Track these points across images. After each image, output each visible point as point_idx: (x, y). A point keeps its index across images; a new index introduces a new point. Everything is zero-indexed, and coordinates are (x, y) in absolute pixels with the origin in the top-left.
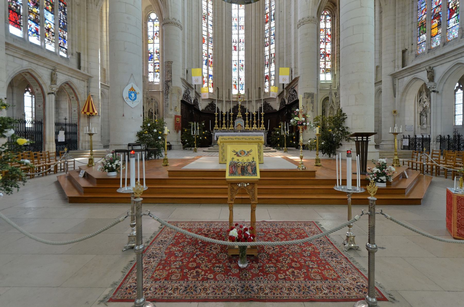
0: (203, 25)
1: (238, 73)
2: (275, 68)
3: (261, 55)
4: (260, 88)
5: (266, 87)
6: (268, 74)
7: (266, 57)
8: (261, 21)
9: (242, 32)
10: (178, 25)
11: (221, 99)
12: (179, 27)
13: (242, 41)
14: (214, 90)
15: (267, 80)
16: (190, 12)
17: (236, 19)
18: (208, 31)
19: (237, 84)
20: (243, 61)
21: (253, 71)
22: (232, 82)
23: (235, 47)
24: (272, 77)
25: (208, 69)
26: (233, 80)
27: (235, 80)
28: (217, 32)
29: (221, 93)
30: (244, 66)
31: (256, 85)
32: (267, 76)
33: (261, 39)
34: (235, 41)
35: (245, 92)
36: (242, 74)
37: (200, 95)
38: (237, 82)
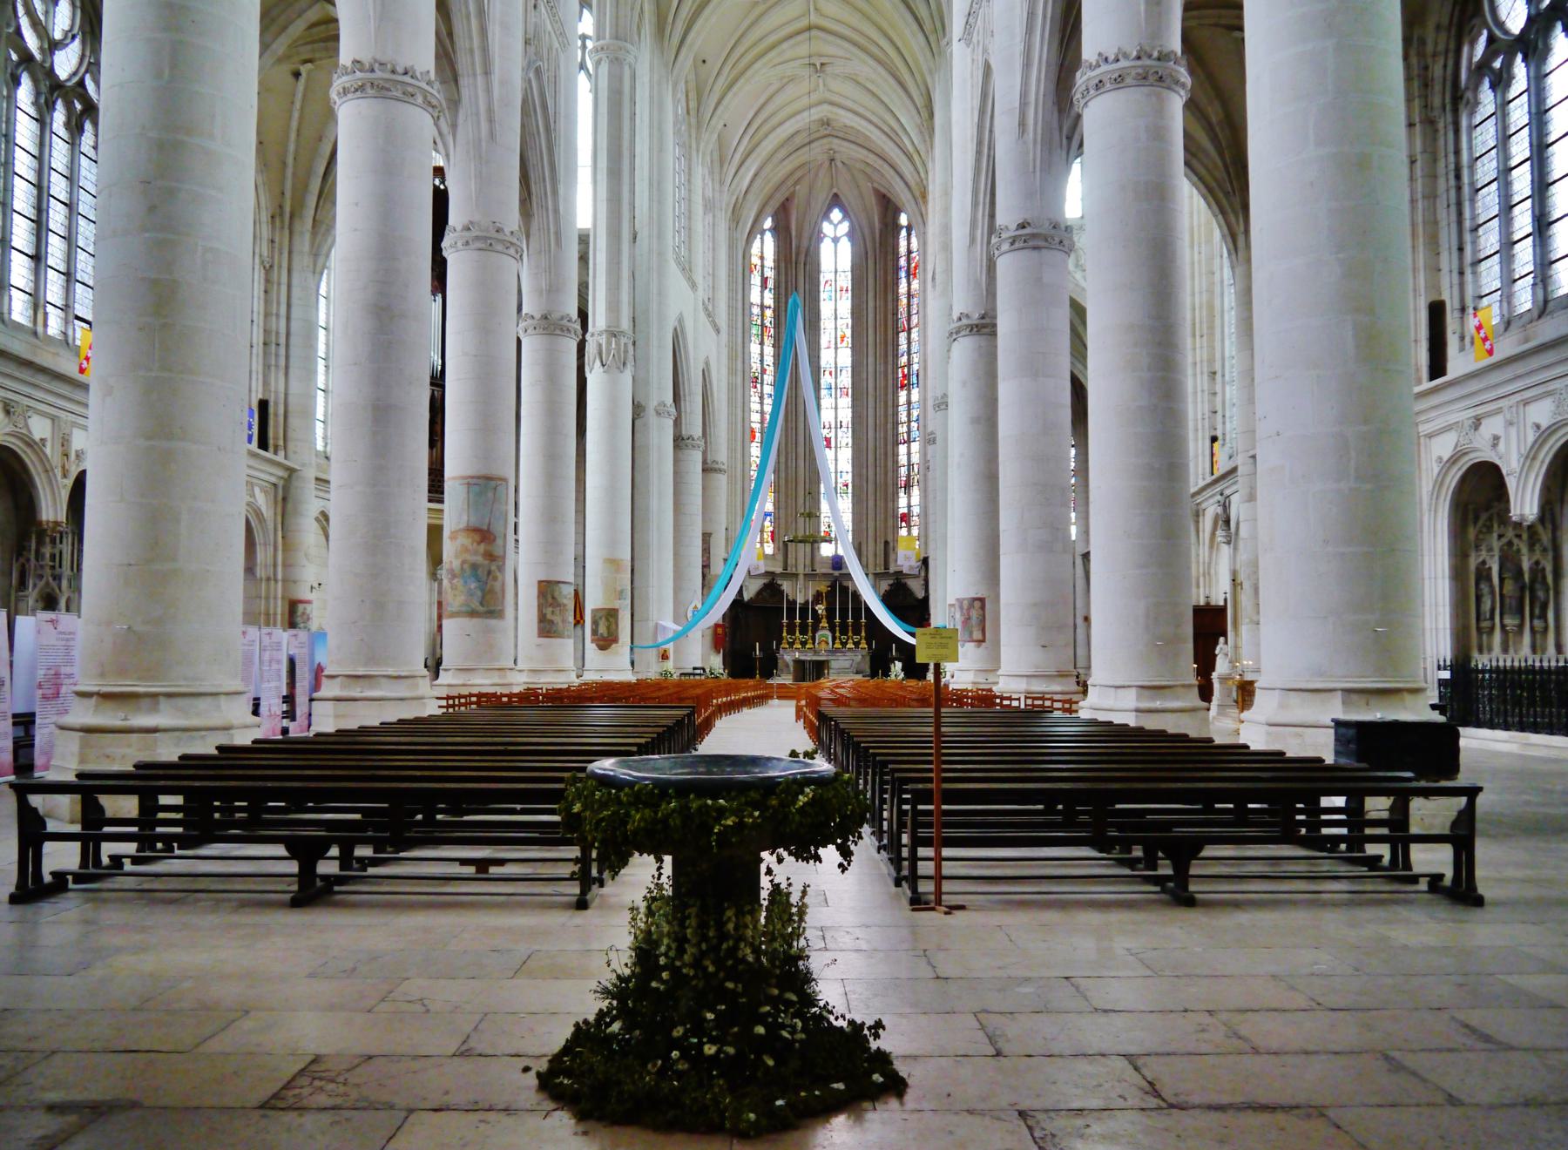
0: (753, 399)
3: (890, 463)
4: (886, 543)
6: (905, 511)
8: (890, 382)
9: (846, 402)
11: (794, 571)
13: (844, 424)
14: (777, 549)
17: (831, 373)
21: (871, 503)
24: (914, 518)
27: (827, 519)
33: (890, 426)
34: (827, 426)
36: (845, 505)
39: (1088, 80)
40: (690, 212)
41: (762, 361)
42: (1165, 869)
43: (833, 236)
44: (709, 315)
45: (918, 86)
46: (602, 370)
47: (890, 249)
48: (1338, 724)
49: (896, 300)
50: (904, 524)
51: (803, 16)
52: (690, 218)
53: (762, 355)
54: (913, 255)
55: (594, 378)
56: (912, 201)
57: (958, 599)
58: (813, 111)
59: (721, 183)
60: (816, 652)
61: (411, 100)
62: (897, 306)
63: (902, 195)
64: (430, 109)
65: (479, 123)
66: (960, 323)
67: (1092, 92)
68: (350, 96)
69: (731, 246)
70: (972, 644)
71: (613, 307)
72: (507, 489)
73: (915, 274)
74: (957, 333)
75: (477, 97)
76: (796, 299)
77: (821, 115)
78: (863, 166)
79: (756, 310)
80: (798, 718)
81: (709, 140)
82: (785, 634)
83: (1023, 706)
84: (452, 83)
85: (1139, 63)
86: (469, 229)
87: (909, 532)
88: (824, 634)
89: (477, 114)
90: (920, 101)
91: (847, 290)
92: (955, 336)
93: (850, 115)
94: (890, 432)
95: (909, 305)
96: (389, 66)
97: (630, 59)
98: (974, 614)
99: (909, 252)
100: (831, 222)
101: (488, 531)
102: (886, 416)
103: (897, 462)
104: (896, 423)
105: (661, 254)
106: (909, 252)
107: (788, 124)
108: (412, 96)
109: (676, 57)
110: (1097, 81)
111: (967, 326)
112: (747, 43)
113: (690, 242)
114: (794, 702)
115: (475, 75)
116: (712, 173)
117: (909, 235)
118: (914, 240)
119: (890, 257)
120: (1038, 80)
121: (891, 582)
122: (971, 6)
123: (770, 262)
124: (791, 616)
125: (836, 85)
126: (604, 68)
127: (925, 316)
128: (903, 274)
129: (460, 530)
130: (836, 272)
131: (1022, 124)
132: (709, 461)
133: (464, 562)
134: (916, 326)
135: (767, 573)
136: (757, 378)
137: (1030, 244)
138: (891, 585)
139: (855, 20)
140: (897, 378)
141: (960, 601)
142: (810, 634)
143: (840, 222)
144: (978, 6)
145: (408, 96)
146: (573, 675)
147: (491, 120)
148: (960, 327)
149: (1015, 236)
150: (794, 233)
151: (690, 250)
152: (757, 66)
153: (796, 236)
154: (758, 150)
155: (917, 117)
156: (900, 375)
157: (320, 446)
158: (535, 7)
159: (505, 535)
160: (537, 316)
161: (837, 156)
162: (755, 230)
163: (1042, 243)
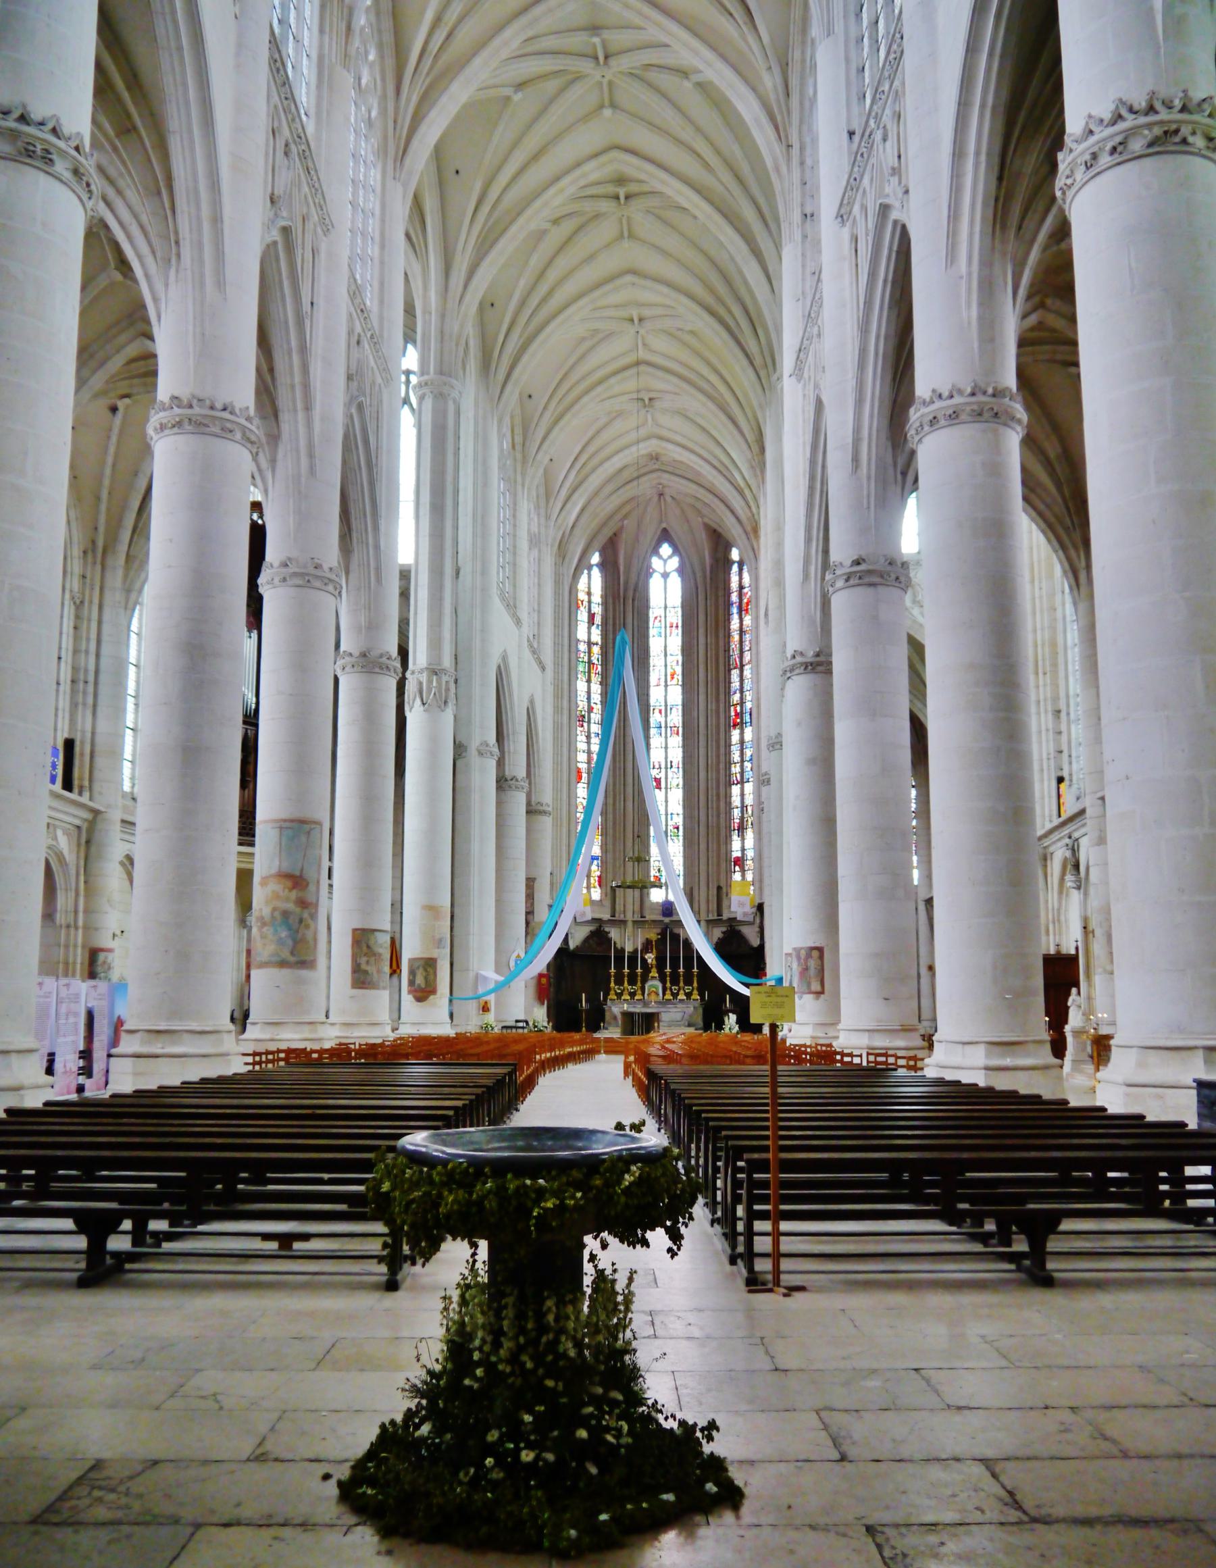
0: (579, 738)
3: (722, 805)
4: (719, 888)
6: (739, 854)
7: (735, 810)
9: (676, 742)
10: (545, 812)
11: (622, 917)
14: (605, 894)
17: (660, 712)
21: (703, 846)
24: (748, 862)
27: (657, 863)
33: (722, 766)
34: (657, 766)
36: (676, 849)
39: (922, 416)
40: (515, 547)
41: (589, 698)
42: (1021, 1245)
43: (662, 571)
44: (534, 652)
45: (748, 420)
46: (422, 708)
47: (721, 586)
48: (1201, 1085)
49: (728, 635)
50: (737, 868)
51: (631, 351)
52: (515, 554)
53: (589, 693)
54: (745, 590)
55: (414, 716)
56: (744, 537)
57: (795, 949)
58: (641, 445)
59: (548, 517)
60: (646, 1004)
61: (229, 435)
62: (729, 642)
63: (732, 529)
64: (249, 445)
65: (299, 459)
66: (794, 661)
67: (926, 428)
68: (167, 432)
69: (558, 582)
70: (812, 996)
71: (435, 644)
72: (321, 833)
73: (747, 610)
74: (792, 670)
75: (297, 431)
76: (624, 636)
77: (650, 450)
78: (690, 501)
79: (583, 647)
80: (626, 1074)
81: (535, 475)
82: (612, 985)
83: (865, 1064)
84: (273, 418)
85: (973, 399)
86: (287, 565)
87: (743, 876)
88: (654, 984)
89: (298, 451)
90: (750, 437)
91: (677, 627)
92: (788, 675)
93: (679, 449)
94: (722, 772)
95: (741, 642)
96: (208, 403)
97: (455, 394)
98: (812, 964)
99: (741, 587)
100: (660, 557)
101: (301, 876)
102: (718, 756)
103: (730, 803)
104: (729, 763)
105: (485, 590)
106: (741, 587)
107: (615, 459)
108: (231, 431)
109: (502, 392)
110: (931, 417)
111: (802, 664)
112: (574, 377)
113: (515, 578)
114: (621, 1058)
115: (295, 410)
116: (537, 507)
117: (741, 570)
118: (746, 575)
119: (721, 593)
120: (871, 416)
121: (724, 929)
122: (802, 342)
123: (597, 597)
124: (619, 965)
125: (666, 420)
126: (428, 403)
127: (758, 653)
128: (735, 610)
129: (271, 876)
130: (666, 607)
131: (856, 460)
132: (533, 803)
133: (274, 909)
134: (749, 663)
135: (594, 920)
136: (583, 716)
137: (866, 580)
138: (723, 933)
139: (685, 355)
140: (730, 717)
141: (797, 951)
142: (639, 984)
143: (670, 557)
144: (809, 342)
145: (226, 432)
146: (388, 1030)
147: (311, 455)
148: (793, 665)
149: (851, 573)
150: (622, 569)
151: (515, 586)
152: (585, 399)
153: (624, 572)
154: (585, 485)
155: (748, 453)
156: (733, 713)
157: (127, 787)
158: (358, 343)
159: (318, 882)
160: (356, 653)
161: (667, 491)
162: (583, 564)
163: (876, 579)
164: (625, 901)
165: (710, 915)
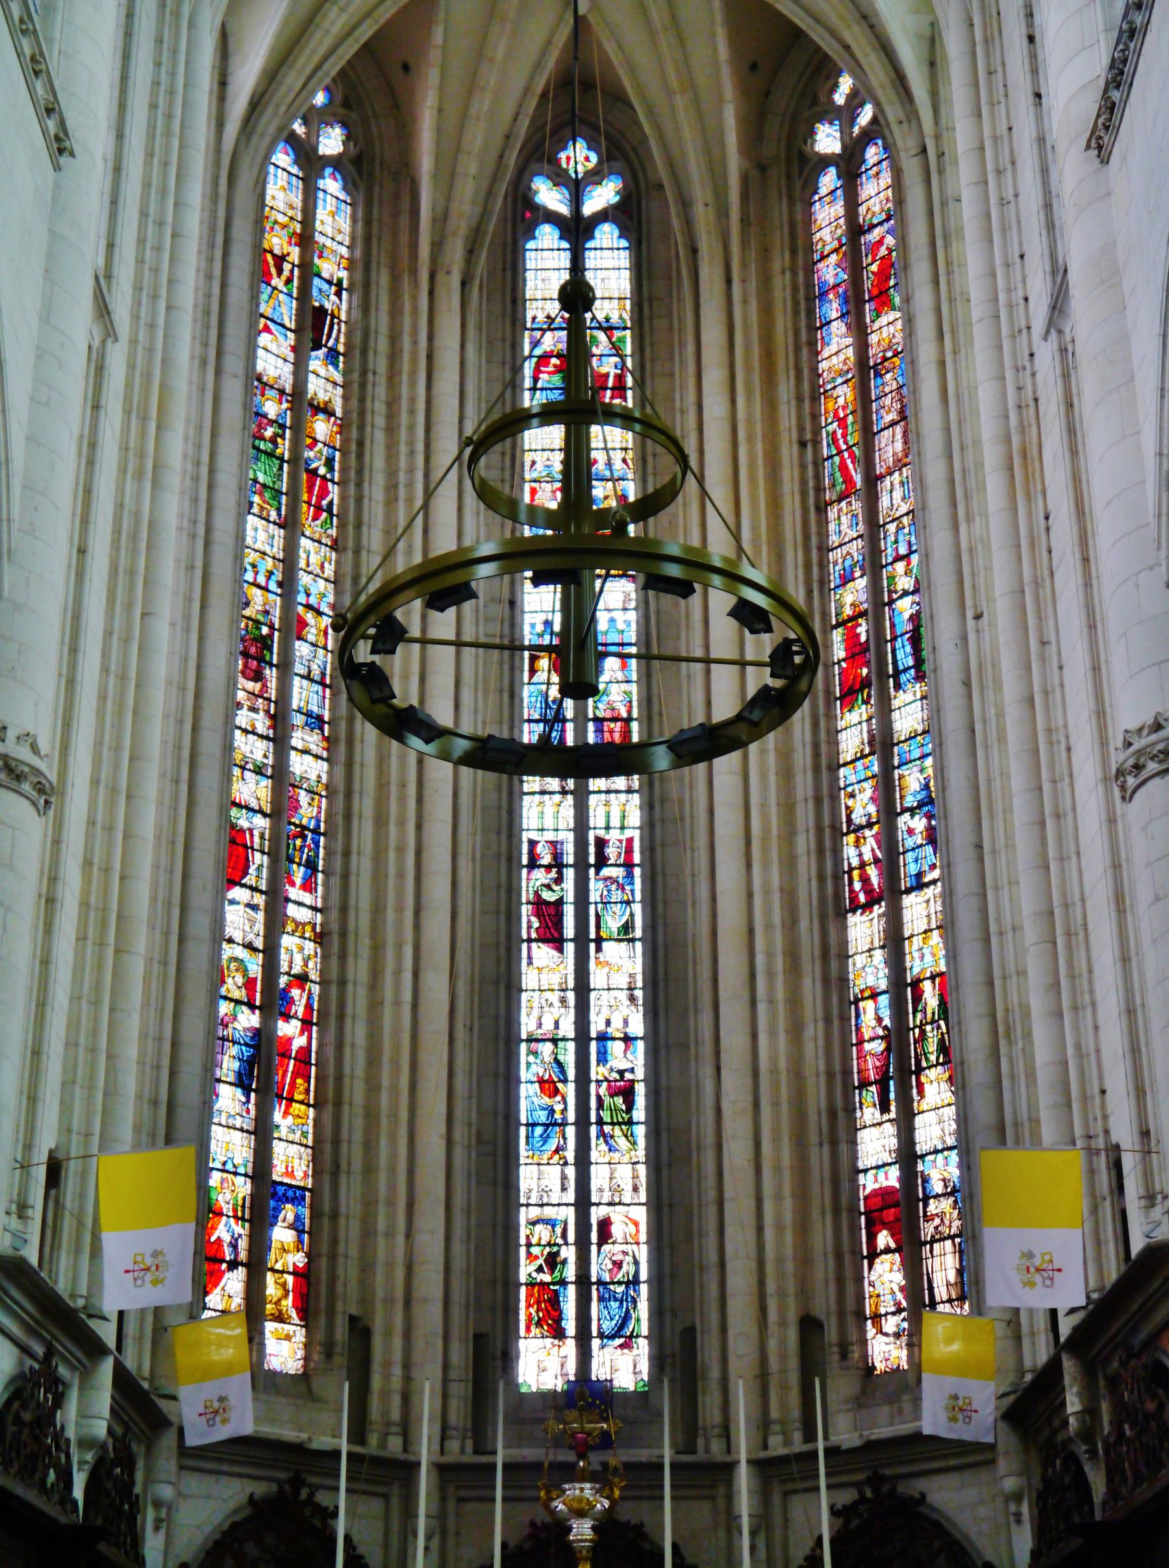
0: (243, 718)
1: (583, 1163)
2: (963, 1120)
5: (877, 1318)
6: (892, 1178)
7: (868, 1006)
12: (26, 787)
13: (611, 852)
15: (884, 1239)
16: (126, 640)
18: (280, 776)
19: (570, 1273)
20: (627, 1040)
22: (511, 1264)
23: (550, 914)
24: (933, 1207)
25: (262, 1133)
26: (523, 1232)
27: (542, 1233)
28: (370, 775)
29: (396, 1382)
30: (640, 1089)
31: (771, 1287)
32: (884, 1193)
33: (804, 843)
35: (658, 1361)
37: (163, 1404)
38: (569, 1253)
50: (884, 1239)
53: (289, 561)
62: (815, 417)
94: (806, 867)
95: (864, 399)
100: (559, 177)
106: (856, 229)
128: (832, 309)
134: (899, 464)
136: (265, 643)
143: (596, 176)
150: (426, 164)
153: (435, 177)
164: (407, 1379)
165: (775, 1441)
